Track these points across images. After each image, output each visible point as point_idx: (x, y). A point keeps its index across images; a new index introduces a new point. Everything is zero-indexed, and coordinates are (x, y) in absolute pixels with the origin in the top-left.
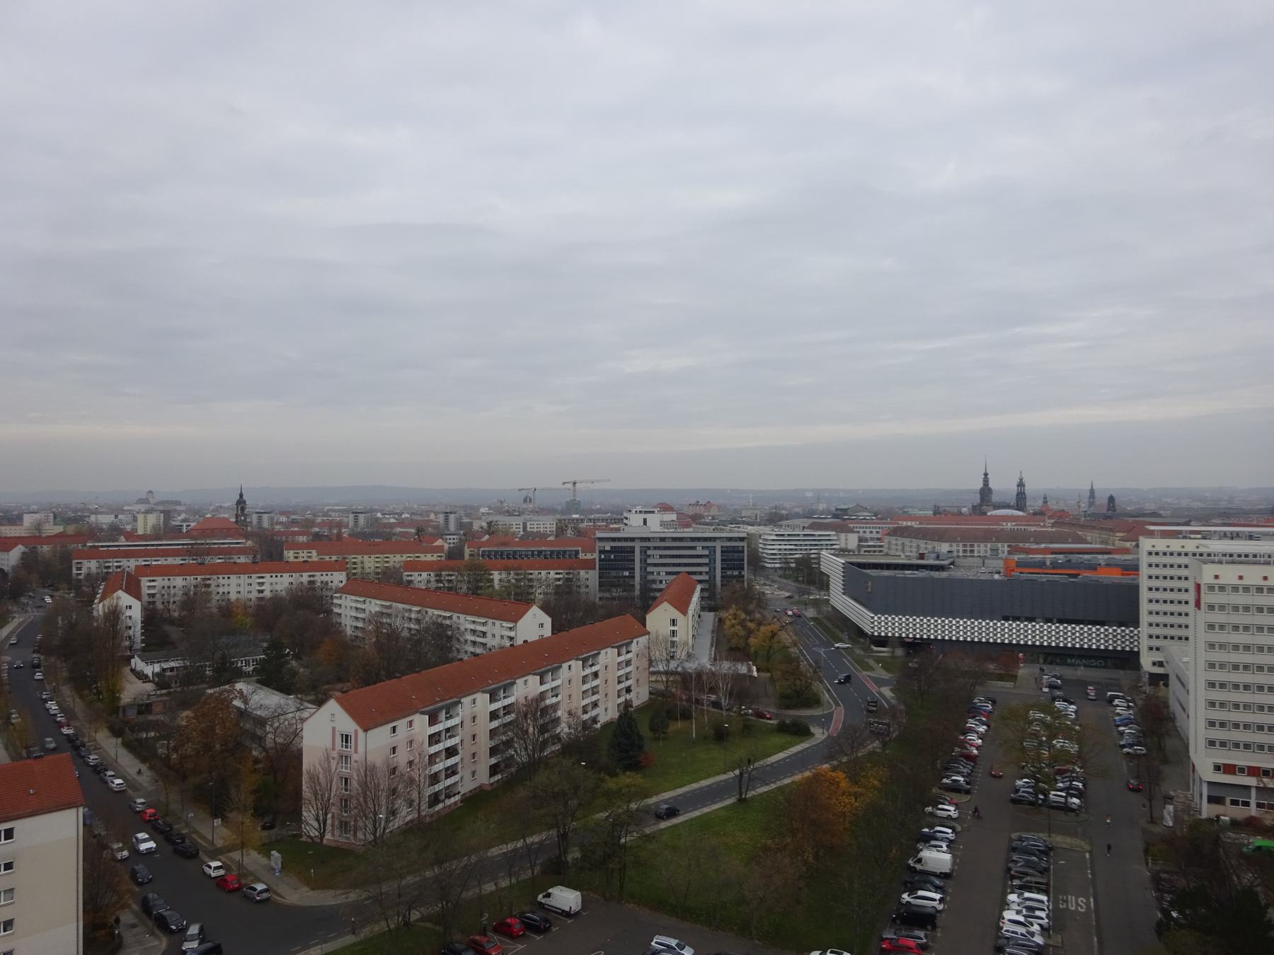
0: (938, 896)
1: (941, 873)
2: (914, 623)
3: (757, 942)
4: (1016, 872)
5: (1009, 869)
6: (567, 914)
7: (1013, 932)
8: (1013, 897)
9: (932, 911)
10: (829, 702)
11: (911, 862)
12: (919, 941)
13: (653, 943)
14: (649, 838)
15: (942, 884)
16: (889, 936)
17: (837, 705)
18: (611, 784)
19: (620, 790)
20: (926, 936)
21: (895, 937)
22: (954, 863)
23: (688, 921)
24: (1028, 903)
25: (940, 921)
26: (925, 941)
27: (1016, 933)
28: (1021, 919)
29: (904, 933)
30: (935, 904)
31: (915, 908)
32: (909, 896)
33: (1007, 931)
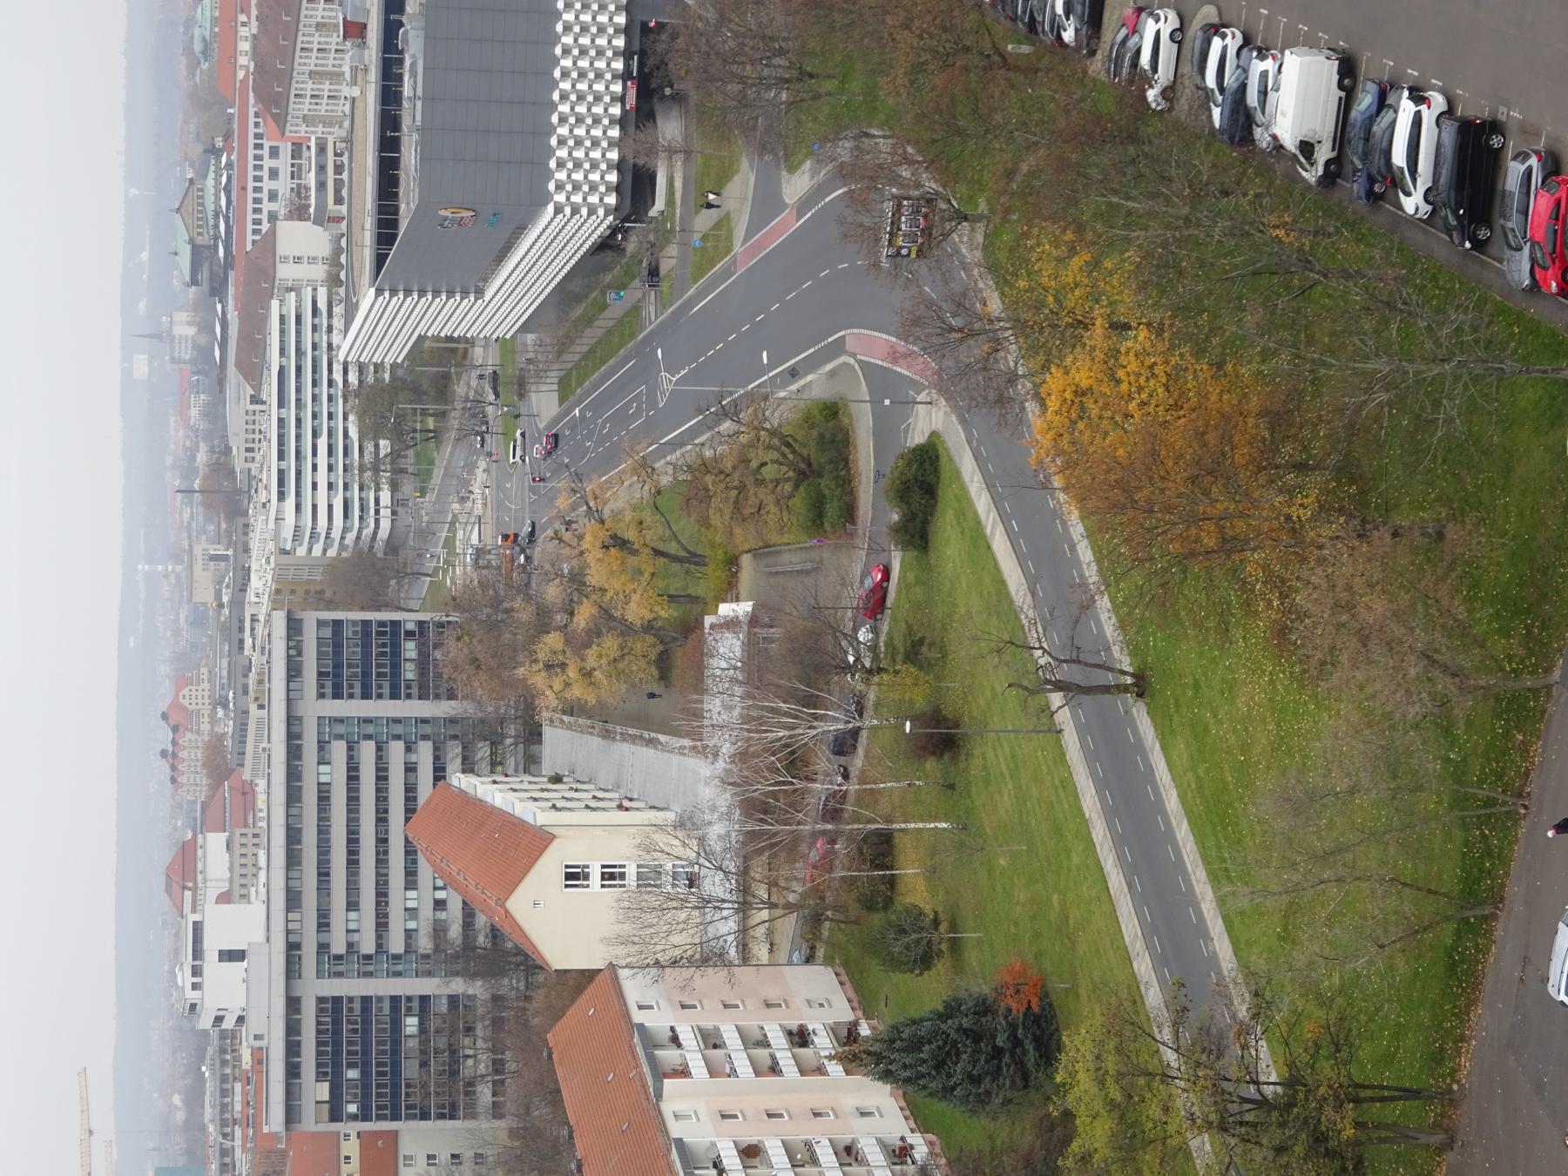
0: (1407, 108)
1: (1341, 86)
2: (570, 165)
3: (1556, 674)
9: (1450, 130)
10: (832, 374)
11: (1311, 175)
12: (1536, 178)
14: (1262, 1006)
15: (1372, 88)
16: (1526, 266)
17: (839, 348)
19: (1112, 1105)
20: (1521, 156)
21: (1527, 249)
22: (1311, 43)
23: (1503, 886)
25: (1476, 108)
29: (1513, 223)
30: (1428, 116)
32: (1408, 194)
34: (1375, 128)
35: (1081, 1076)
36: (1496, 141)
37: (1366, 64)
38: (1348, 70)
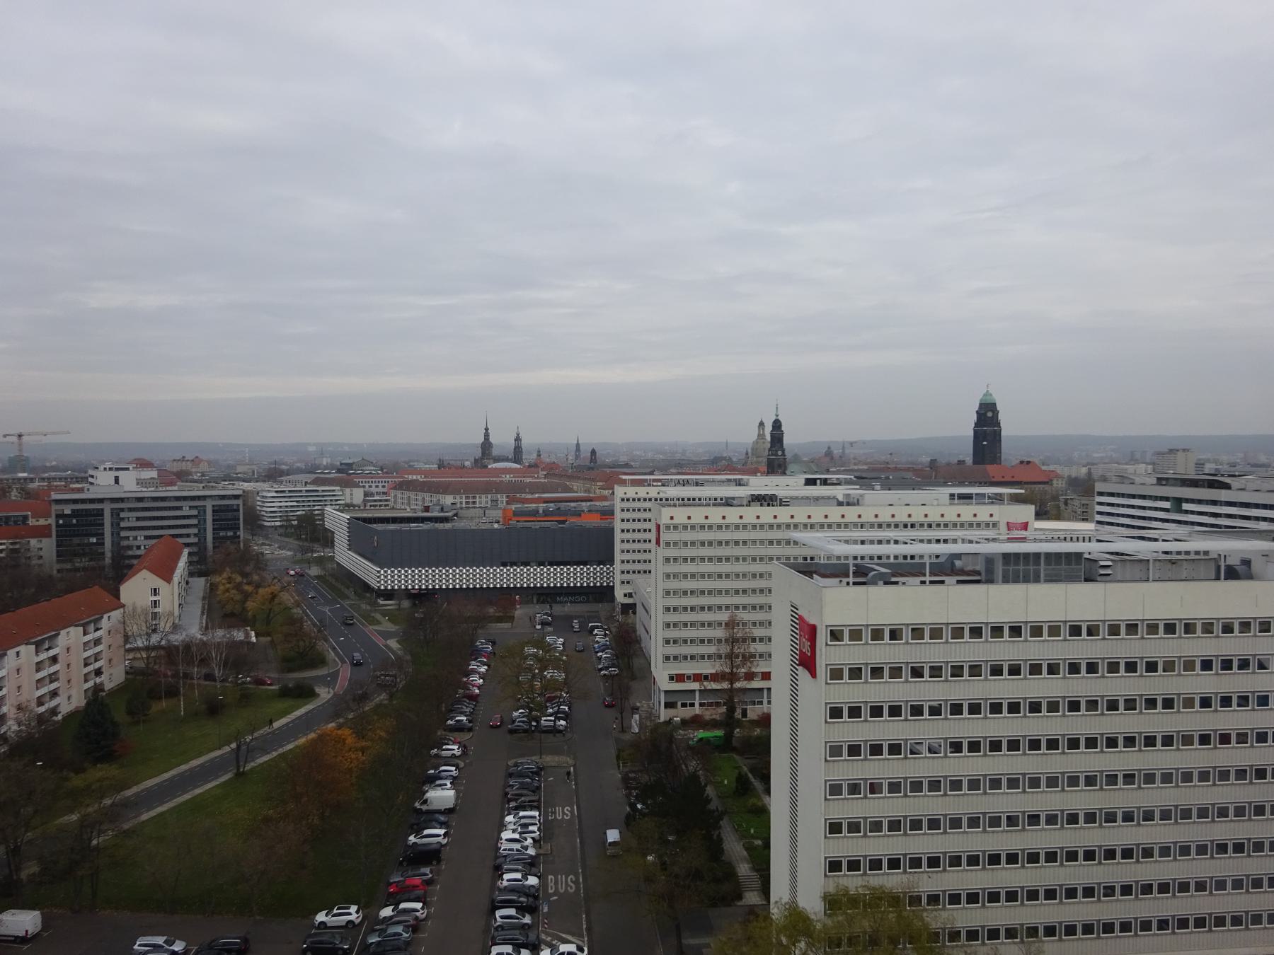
0: (442, 832)
1: (446, 809)
3: (258, 918)
4: (512, 795)
5: (506, 794)
6: (23, 940)
7: (509, 850)
8: (509, 818)
10: (335, 660)
11: (417, 805)
12: (425, 878)
13: (136, 947)
14: (127, 834)
16: (397, 880)
17: (343, 662)
18: (77, 781)
20: (431, 872)
22: (457, 798)
24: (523, 821)
26: (430, 876)
27: (512, 850)
28: (516, 836)
30: (439, 839)
31: (420, 848)
32: (415, 837)
33: (505, 850)
34: (434, 823)
35: (101, 773)
36: (434, 863)
37: (454, 816)
38: (449, 811)
